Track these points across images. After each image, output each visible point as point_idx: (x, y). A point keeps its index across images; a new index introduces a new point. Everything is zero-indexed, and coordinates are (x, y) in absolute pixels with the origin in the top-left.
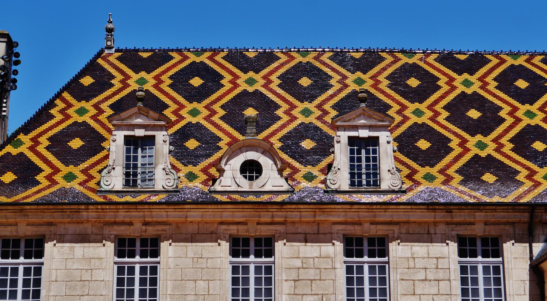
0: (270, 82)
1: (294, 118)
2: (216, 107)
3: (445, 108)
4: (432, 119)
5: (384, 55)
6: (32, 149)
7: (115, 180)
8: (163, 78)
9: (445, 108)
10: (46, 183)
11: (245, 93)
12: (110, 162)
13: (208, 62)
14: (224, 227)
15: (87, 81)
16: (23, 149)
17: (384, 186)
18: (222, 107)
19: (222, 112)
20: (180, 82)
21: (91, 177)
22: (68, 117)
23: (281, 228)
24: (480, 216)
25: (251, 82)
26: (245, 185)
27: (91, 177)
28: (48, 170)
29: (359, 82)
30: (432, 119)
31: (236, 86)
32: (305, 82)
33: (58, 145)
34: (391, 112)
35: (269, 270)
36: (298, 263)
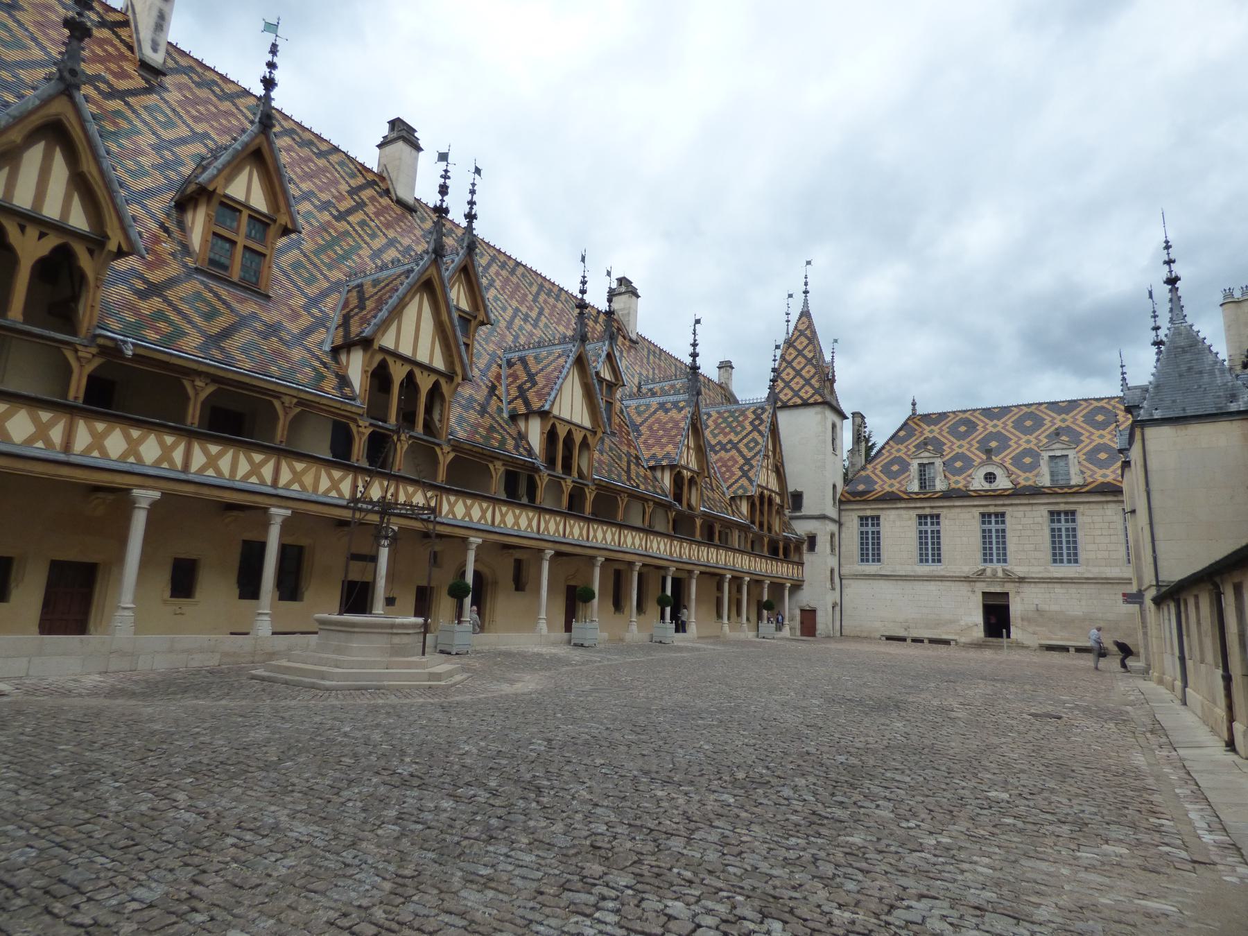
2: (974, 443)
7: (915, 487)
14: (974, 510)
15: (902, 433)
16: (869, 472)
17: (1073, 483)
23: (1010, 509)
25: (995, 426)
26: (987, 486)
29: (1064, 420)
32: (1028, 423)
33: (886, 470)
35: (1004, 531)
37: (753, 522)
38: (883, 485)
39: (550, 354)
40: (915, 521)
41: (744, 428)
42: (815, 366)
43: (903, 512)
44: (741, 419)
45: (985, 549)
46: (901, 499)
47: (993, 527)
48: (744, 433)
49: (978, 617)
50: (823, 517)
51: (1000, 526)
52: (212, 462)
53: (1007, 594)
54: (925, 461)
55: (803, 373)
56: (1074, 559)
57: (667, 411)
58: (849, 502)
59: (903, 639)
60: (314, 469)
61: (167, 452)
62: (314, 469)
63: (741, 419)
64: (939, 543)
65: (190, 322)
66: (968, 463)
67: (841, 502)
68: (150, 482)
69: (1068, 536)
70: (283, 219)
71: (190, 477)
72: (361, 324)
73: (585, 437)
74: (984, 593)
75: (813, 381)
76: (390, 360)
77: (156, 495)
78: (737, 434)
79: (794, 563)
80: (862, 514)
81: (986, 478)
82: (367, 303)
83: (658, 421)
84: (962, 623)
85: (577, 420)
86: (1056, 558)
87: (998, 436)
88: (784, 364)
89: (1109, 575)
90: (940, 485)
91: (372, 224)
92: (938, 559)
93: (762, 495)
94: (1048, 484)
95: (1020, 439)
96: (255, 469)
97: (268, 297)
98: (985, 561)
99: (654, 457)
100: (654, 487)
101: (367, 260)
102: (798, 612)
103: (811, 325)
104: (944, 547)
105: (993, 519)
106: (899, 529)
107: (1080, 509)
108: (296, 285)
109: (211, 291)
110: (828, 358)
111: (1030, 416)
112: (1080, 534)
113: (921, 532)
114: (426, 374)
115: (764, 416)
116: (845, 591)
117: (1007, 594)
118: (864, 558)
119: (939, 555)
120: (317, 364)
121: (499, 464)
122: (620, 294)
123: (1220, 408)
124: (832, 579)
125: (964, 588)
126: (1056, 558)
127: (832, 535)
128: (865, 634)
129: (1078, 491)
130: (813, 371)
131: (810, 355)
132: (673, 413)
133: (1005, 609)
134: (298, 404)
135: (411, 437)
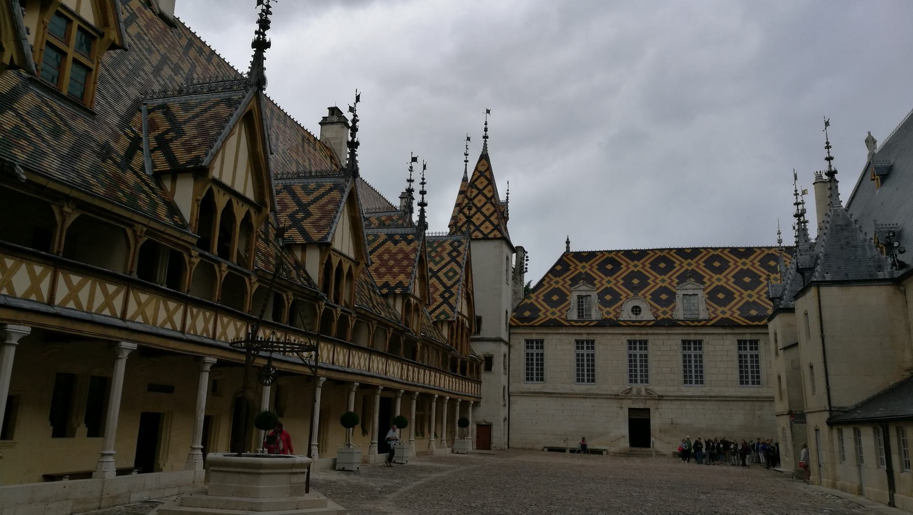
1: (657, 284)
2: (619, 279)
3: (733, 277)
4: (726, 283)
6: (536, 300)
7: (574, 315)
9: (733, 277)
10: (543, 316)
12: (571, 306)
14: (623, 337)
17: (701, 317)
20: (601, 267)
21: (562, 314)
22: (551, 285)
24: (748, 331)
26: (634, 317)
27: (562, 314)
28: (544, 311)
30: (726, 283)
31: (628, 268)
32: (662, 265)
33: (547, 298)
34: (705, 280)
35: (646, 356)
36: (660, 353)
37: (451, 345)
38: (546, 313)
39: (319, 186)
40: (573, 346)
41: (443, 259)
42: (493, 205)
43: (563, 337)
44: (439, 249)
45: (631, 371)
46: (562, 326)
47: (638, 352)
48: (443, 263)
49: (625, 431)
50: (499, 340)
51: (643, 352)
52: (73, 293)
53: (649, 409)
54: (584, 294)
55: (484, 210)
56: (700, 381)
57: (396, 243)
58: (518, 326)
59: (562, 450)
60: (154, 300)
61: (36, 281)
62: (154, 300)
63: (439, 249)
64: (593, 365)
65: (44, 140)
66: (616, 297)
67: (511, 327)
68: (22, 316)
70: (113, 35)
71: (57, 310)
72: (189, 151)
73: (350, 267)
74: (630, 409)
75: (493, 218)
76: (215, 189)
77: (26, 330)
78: (436, 264)
79: (472, 381)
80: (529, 337)
81: (633, 311)
82: (185, 128)
83: (388, 251)
85: (345, 252)
86: (687, 380)
87: (638, 275)
88: (466, 201)
89: (727, 394)
90: (595, 315)
91: (146, 38)
93: (458, 321)
95: (657, 278)
96: (108, 303)
97: (93, 114)
98: (631, 381)
99: (386, 285)
100: (389, 313)
101: (151, 76)
102: (475, 427)
103: (489, 168)
104: (597, 369)
105: (638, 346)
106: (560, 351)
107: (706, 339)
108: (108, 102)
109: (48, 105)
110: (502, 198)
111: (663, 259)
112: (705, 360)
113: (578, 355)
114: (240, 204)
115: (461, 249)
116: (513, 407)
117: (649, 409)
118: (529, 378)
119: (593, 375)
120: (146, 188)
121: (290, 294)
122: (332, 123)
123: (871, 276)
124: (504, 396)
125: (613, 405)
126: (687, 380)
127: (505, 356)
128: (529, 446)
130: (492, 209)
131: (489, 195)
132: (403, 245)
133: (647, 422)
134: (147, 233)
135: (229, 267)
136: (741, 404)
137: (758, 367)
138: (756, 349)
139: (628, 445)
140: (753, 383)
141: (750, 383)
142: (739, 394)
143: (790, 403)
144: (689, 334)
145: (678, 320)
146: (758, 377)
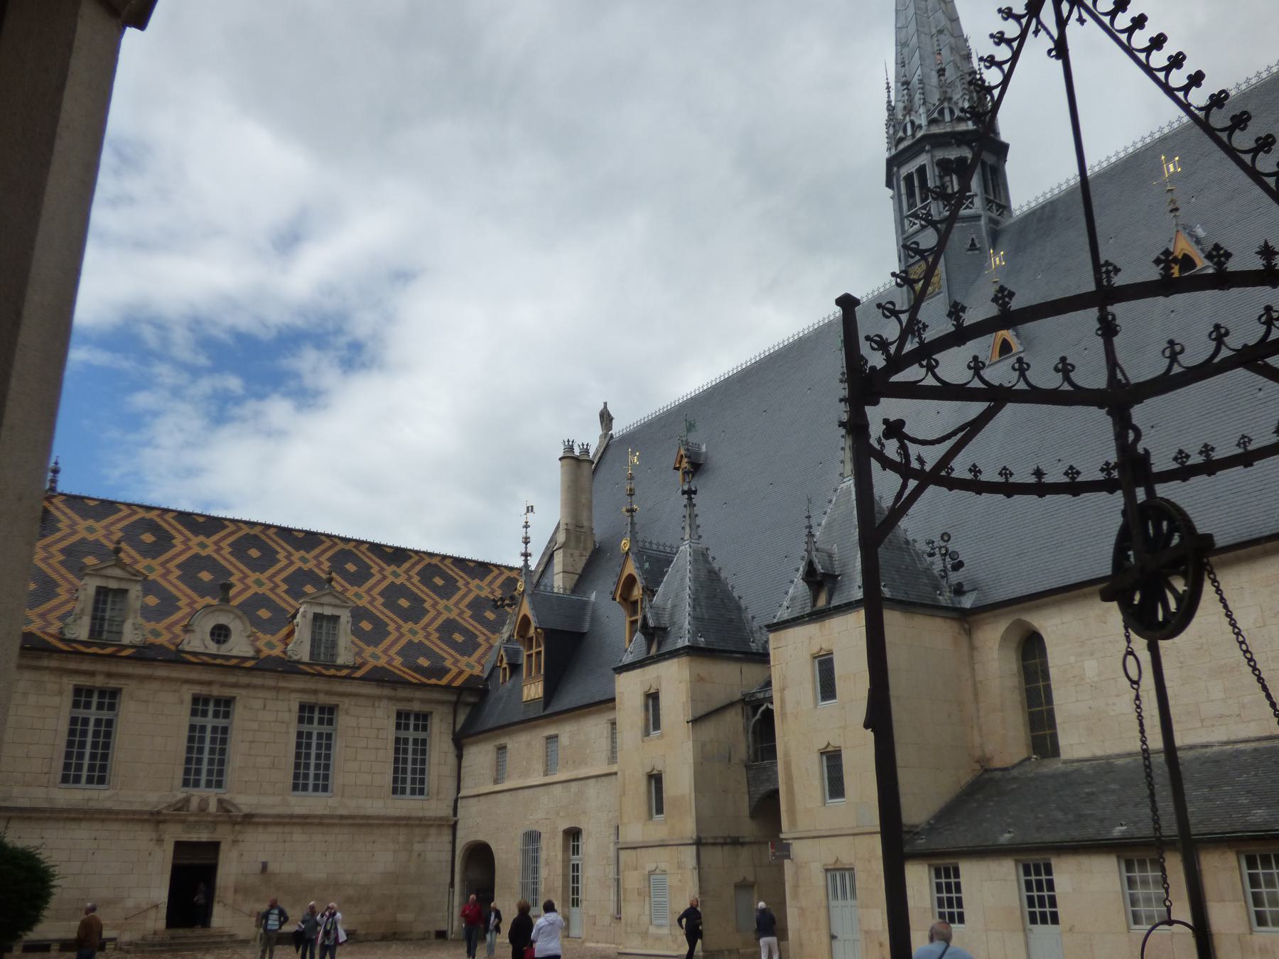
0: (221, 549)
5: (323, 538)
7: (82, 631)
8: (113, 528)
11: (196, 556)
13: (158, 520)
14: (185, 687)
17: (340, 661)
18: (178, 566)
19: (178, 573)
23: (244, 692)
24: (419, 694)
26: (213, 648)
36: (255, 726)
40: (68, 699)
45: (188, 760)
49: (160, 893)
51: (221, 722)
54: (113, 585)
64: (107, 746)
69: (319, 746)
74: (178, 845)
81: (212, 634)
84: (130, 903)
86: (299, 784)
89: (369, 812)
90: (131, 634)
92: (99, 776)
94: (306, 659)
95: (246, 576)
98: (186, 783)
107: (345, 703)
113: (74, 721)
119: (103, 768)
125: (142, 837)
126: (299, 784)
129: (350, 674)
136: (392, 831)
137: (423, 762)
138: (425, 728)
139: (162, 924)
140: (413, 792)
141: (408, 791)
142: (391, 812)
143: (699, 821)
144: (315, 692)
145: (299, 662)
146: (422, 781)
